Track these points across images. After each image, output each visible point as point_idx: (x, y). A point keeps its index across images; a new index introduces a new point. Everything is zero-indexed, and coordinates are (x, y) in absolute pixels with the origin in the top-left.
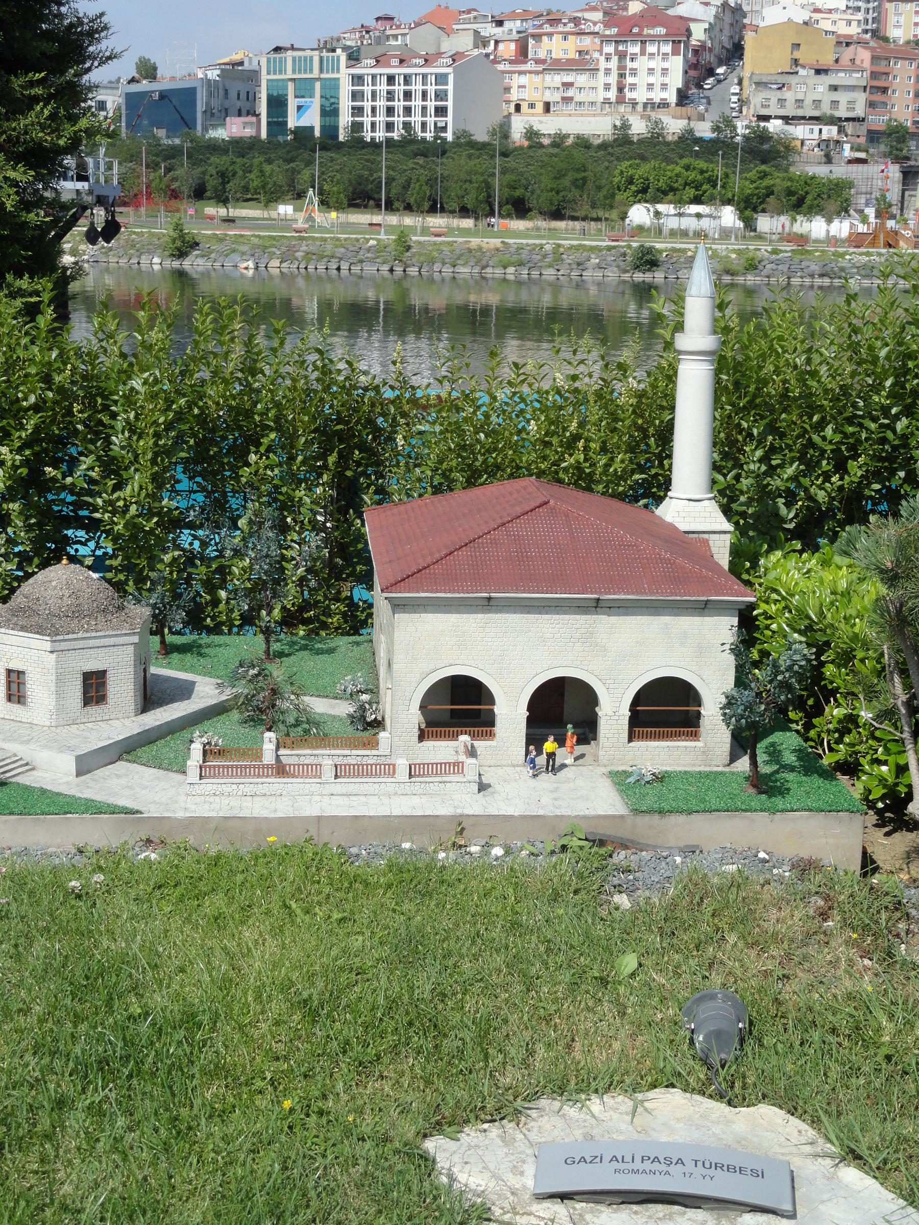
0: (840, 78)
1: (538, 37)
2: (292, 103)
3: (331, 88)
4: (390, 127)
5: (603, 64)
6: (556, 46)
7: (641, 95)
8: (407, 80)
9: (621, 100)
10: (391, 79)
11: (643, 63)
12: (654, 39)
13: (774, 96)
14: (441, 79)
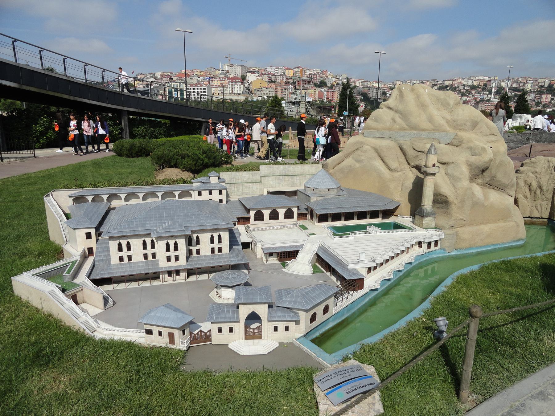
0: (270, 89)
1: (212, 81)
2: (174, 93)
3: (182, 91)
4: (194, 98)
5: (229, 86)
6: (215, 83)
7: (236, 92)
8: (197, 89)
9: (232, 93)
10: (194, 89)
11: (236, 86)
12: (238, 82)
13: (260, 93)
14: (204, 89)
